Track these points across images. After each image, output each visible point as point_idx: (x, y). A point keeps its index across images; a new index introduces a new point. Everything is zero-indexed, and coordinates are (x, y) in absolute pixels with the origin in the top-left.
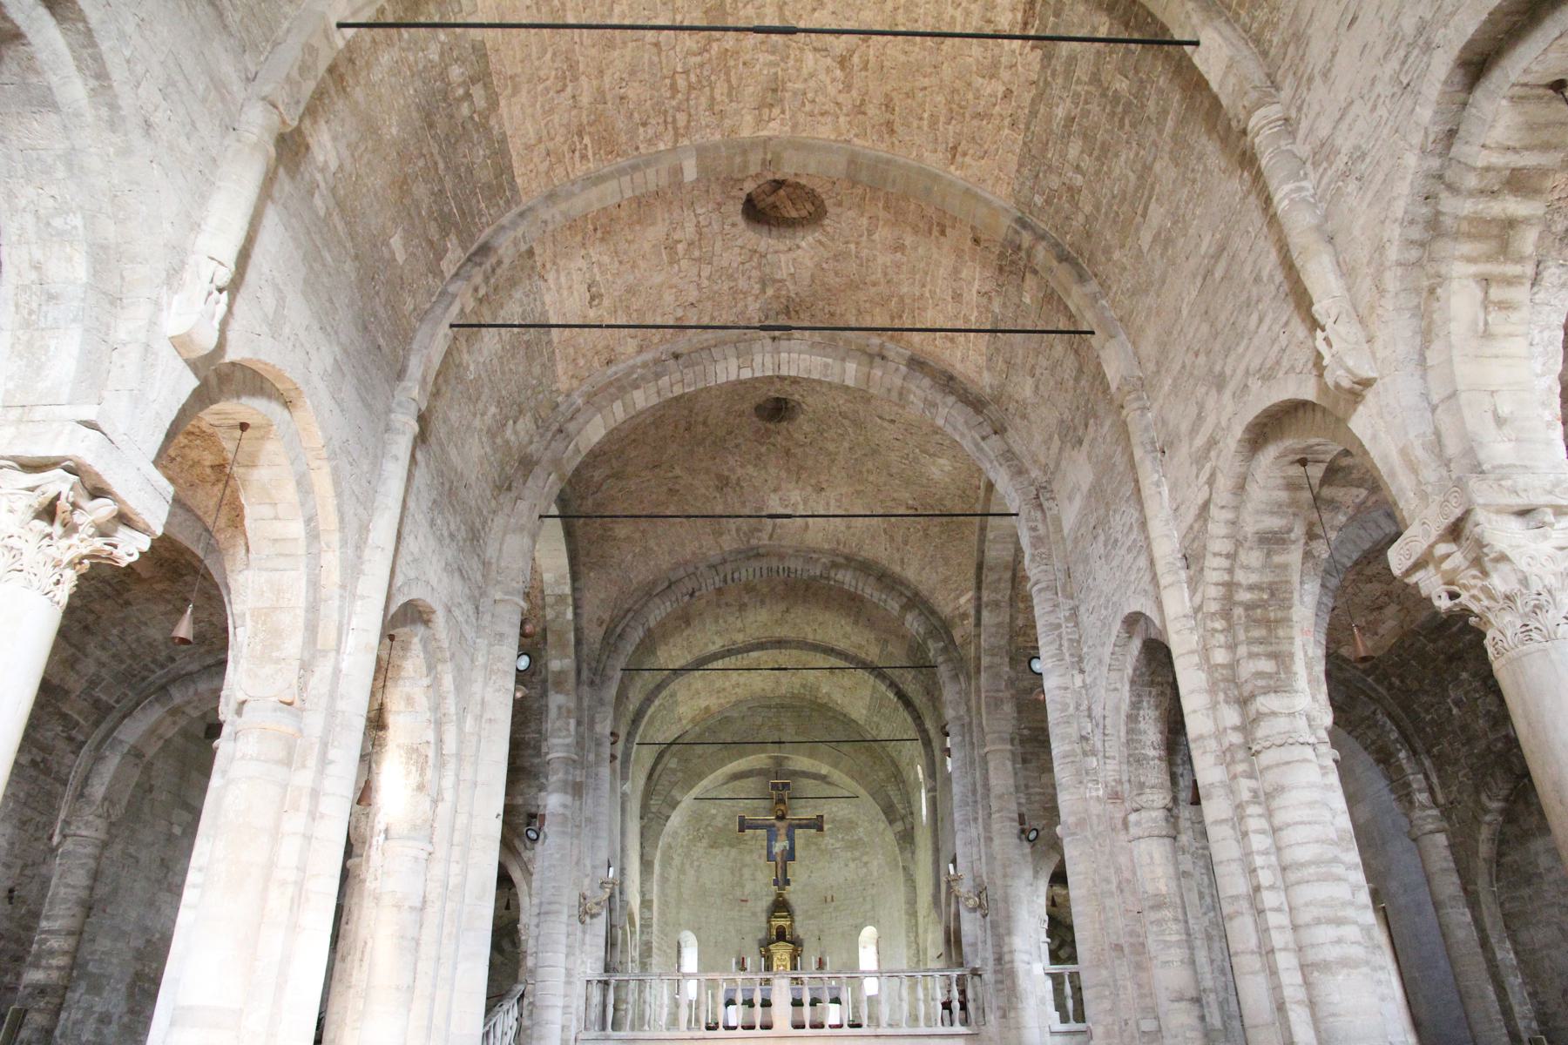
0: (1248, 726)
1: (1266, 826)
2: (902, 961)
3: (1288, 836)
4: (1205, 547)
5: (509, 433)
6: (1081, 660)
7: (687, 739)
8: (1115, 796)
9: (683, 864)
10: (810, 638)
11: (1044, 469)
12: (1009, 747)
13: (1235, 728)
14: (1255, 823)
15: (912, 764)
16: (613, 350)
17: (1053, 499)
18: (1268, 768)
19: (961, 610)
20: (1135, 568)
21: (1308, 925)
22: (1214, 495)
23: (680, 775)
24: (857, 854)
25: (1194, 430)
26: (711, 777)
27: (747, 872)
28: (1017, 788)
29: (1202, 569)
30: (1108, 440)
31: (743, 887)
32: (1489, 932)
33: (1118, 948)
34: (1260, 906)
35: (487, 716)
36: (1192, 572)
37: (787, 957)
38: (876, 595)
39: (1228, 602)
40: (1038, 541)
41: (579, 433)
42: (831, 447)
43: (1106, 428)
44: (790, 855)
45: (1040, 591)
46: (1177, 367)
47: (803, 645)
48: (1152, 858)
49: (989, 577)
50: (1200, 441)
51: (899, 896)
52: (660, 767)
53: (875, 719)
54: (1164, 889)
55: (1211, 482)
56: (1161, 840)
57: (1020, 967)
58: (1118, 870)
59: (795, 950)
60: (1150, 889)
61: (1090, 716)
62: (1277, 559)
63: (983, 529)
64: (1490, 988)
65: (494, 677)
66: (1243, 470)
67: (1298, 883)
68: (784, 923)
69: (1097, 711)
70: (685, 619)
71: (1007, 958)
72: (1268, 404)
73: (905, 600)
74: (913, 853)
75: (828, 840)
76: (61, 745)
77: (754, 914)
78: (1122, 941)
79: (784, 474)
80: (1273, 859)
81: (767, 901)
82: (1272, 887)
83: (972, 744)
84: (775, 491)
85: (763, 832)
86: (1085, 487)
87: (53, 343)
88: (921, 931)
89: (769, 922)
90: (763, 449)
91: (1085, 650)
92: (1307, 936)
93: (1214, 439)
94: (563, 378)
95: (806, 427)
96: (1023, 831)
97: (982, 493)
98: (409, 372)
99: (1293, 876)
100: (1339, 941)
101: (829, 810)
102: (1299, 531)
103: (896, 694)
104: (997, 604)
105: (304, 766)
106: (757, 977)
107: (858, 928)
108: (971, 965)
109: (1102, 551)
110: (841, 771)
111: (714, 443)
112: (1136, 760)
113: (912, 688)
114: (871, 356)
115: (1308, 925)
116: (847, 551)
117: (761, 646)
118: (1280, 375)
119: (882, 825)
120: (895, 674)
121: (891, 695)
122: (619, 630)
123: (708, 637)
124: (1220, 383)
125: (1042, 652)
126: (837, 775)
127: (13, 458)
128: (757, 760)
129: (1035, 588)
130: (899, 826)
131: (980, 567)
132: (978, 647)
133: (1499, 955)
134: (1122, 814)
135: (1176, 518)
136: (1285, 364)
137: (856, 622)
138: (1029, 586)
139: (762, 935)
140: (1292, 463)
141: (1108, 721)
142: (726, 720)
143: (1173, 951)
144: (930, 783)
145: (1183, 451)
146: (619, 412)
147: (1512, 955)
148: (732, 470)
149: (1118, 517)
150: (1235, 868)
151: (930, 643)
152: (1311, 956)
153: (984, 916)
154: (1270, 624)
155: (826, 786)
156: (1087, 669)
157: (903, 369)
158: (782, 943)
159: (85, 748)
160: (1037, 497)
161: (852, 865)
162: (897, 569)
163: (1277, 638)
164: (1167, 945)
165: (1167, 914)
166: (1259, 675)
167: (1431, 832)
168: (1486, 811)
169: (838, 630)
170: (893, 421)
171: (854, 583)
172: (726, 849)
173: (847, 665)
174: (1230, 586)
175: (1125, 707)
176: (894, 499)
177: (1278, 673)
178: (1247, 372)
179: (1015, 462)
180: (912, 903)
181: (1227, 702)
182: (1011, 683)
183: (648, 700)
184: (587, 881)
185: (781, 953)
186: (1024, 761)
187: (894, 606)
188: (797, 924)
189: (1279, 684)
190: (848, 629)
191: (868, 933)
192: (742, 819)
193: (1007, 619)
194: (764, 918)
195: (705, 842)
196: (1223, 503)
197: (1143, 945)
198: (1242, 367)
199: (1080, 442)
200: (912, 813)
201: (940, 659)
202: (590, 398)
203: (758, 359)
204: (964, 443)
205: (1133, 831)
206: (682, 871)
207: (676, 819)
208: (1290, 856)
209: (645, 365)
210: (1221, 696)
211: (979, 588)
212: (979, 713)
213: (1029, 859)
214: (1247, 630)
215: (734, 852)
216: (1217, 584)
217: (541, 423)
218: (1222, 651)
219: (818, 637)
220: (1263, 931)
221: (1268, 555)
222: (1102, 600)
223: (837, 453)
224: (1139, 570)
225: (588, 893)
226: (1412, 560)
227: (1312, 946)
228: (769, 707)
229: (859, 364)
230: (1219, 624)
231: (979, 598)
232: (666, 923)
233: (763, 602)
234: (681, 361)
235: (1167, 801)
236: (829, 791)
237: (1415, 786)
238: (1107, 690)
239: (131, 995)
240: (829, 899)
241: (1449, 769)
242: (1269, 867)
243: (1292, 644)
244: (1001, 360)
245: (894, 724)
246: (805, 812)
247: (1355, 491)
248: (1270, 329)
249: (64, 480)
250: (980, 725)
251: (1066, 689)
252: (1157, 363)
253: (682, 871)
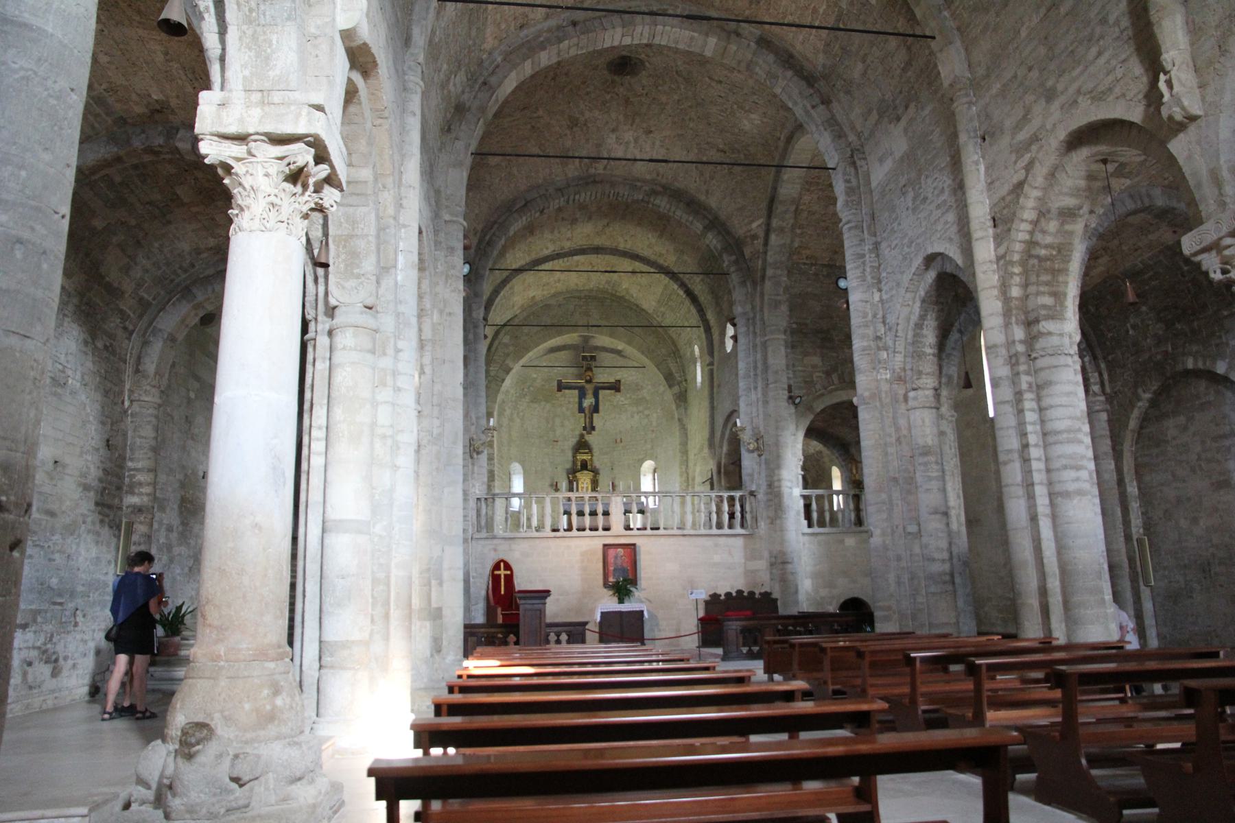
0: (1031, 340)
1: (1036, 407)
2: (676, 485)
3: (1052, 414)
4: (1014, 214)
5: (451, 87)
6: (880, 282)
7: (516, 321)
8: (900, 379)
9: (512, 414)
10: (622, 247)
11: (859, 135)
12: (783, 337)
13: (1021, 342)
14: (1029, 404)
15: (691, 346)
16: (527, 16)
17: (865, 159)
18: (1042, 369)
19: (752, 233)
20: (942, 221)
21: (1058, 470)
22: (1030, 178)
23: (511, 348)
24: (641, 408)
25: (1018, 127)
26: (535, 350)
27: (558, 421)
28: (787, 366)
29: (1009, 230)
30: (927, 122)
31: (554, 431)
32: (1126, 475)
33: (895, 480)
34: (1027, 457)
35: (447, 310)
36: (999, 231)
37: (588, 481)
38: (685, 216)
39: (1028, 254)
40: (850, 191)
41: (499, 86)
42: (664, 99)
43: (926, 112)
44: (596, 409)
45: (850, 229)
46: (1008, 75)
47: (615, 252)
48: (923, 422)
49: (779, 209)
50: (1023, 136)
51: (674, 440)
52: (496, 342)
53: (662, 309)
54: (930, 443)
55: (1029, 168)
56: (930, 410)
57: (785, 490)
58: (898, 429)
59: (595, 476)
60: (921, 442)
61: (884, 322)
62: (1068, 227)
63: (778, 174)
64: (1119, 509)
65: (450, 281)
66: (1057, 162)
67: (1055, 443)
68: (585, 457)
69: (891, 319)
70: (530, 230)
71: (776, 484)
72: (1093, 118)
73: (707, 222)
74: (686, 409)
75: (619, 398)
76: (120, 332)
77: (563, 451)
78: (897, 475)
79: (621, 118)
80: (1038, 427)
81: (573, 441)
82: (1036, 445)
83: (755, 333)
84: (613, 131)
85: (576, 392)
86: (898, 155)
87: (274, 38)
88: (691, 464)
89: (574, 456)
90: (608, 97)
91: (884, 274)
92: (1055, 476)
93: (1036, 136)
94: (490, 39)
95: (644, 82)
96: (790, 398)
97: (781, 144)
98: (414, 40)
99: (1051, 439)
100: (1077, 479)
101: (623, 375)
102: (1085, 209)
103: (685, 292)
104: (781, 230)
105: (385, 354)
106: (587, 496)
107: (641, 462)
108: (749, 489)
109: (910, 205)
110: (634, 347)
111: (571, 90)
112: (918, 355)
113: (698, 286)
114: (729, 33)
115: (1058, 470)
116: (664, 181)
117: (582, 251)
118: (1111, 98)
119: (663, 387)
120: (686, 278)
121: (681, 293)
122: (487, 238)
123: (544, 244)
124: (1050, 96)
125: (849, 274)
126: (630, 350)
127: (265, 134)
128: (571, 338)
129: (846, 227)
130: (676, 389)
131: (772, 201)
132: (765, 261)
133: (1129, 489)
134: (904, 392)
135: (989, 190)
136: (1117, 90)
137: (661, 236)
138: (841, 225)
139: (569, 466)
140: (1097, 161)
141: (900, 327)
142: (547, 306)
143: (933, 482)
144: (708, 359)
145: (1005, 141)
146: (527, 69)
147: (1136, 490)
148: (582, 113)
149: (930, 181)
150: (1012, 432)
151: (725, 257)
152: (1058, 488)
153: (760, 456)
154: (1055, 272)
155: (618, 358)
156: (885, 288)
157: (752, 44)
158: (586, 472)
159: (134, 335)
160: (852, 156)
161: (637, 417)
162: (703, 198)
163: (1058, 282)
164: (930, 479)
165: (932, 459)
166: (1044, 307)
167: (1098, 411)
168: (1139, 399)
169: (645, 241)
170: (720, 82)
171: (668, 206)
172: (543, 403)
173: (652, 270)
174: (1031, 243)
175: (915, 318)
176: (708, 143)
177: (1055, 306)
178: (1079, 92)
179: (836, 128)
180: (684, 444)
181: (1017, 324)
182: (787, 289)
183: (496, 292)
184: (473, 428)
185: (585, 479)
186: (793, 347)
187: (698, 226)
188: (594, 458)
189: (1056, 314)
190: (654, 241)
191: (648, 465)
192: (560, 382)
193: (788, 241)
194: (570, 454)
195: (528, 398)
196: (1037, 185)
197: (912, 478)
198: (1075, 86)
199: (898, 119)
200: (686, 380)
201: (732, 269)
202: (507, 57)
203: (639, 29)
204: (795, 109)
205: (911, 403)
206: (511, 420)
207: (508, 381)
208: (1050, 426)
209: (550, 30)
210: (1014, 319)
211: (769, 216)
212: (762, 310)
213: (794, 417)
214: (1038, 276)
215: (548, 406)
216: (1020, 242)
217: (472, 79)
218: (1018, 288)
219: (628, 246)
220: (1027, 472)
221: (1062, 224)
222: (906, 241)
223: (667, 104)
224: (946, 223)
225: (475, 437)
226: (1202, 246)
227: (1059, 482)
228: (579, 298)
229: (719, 39)
230: (1017, 270)
231: (768, 225)
232: (502, 457)
233: (590, 218)
234: (578, 28)
235: (936, 384)
236: (621, 362)
237: (1092, 380)
238: (902, 305)
239: (181, 513)
241: (1118, 371)
242: (1035, 433)
243: (1066, 287)
244: (837, 46)
245: (680, 314)
246: (602, 377)
247: (1123, 180)
248: (1108, 62)
249: (308, 153)
250: (762, 319)
251: (867, 302)
252: (988, 68)
253: (511, 420)
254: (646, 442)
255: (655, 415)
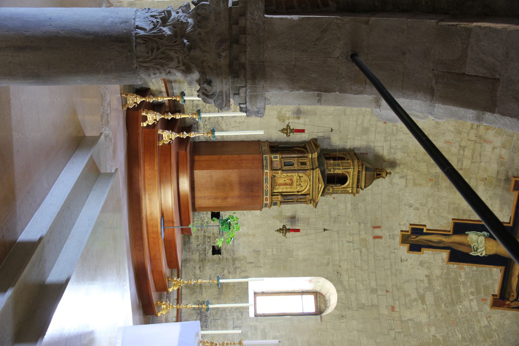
24: (437, 285)
77: (366, 131)
240: (378, 232)
254: (373, 291)
255: (423, 318)
